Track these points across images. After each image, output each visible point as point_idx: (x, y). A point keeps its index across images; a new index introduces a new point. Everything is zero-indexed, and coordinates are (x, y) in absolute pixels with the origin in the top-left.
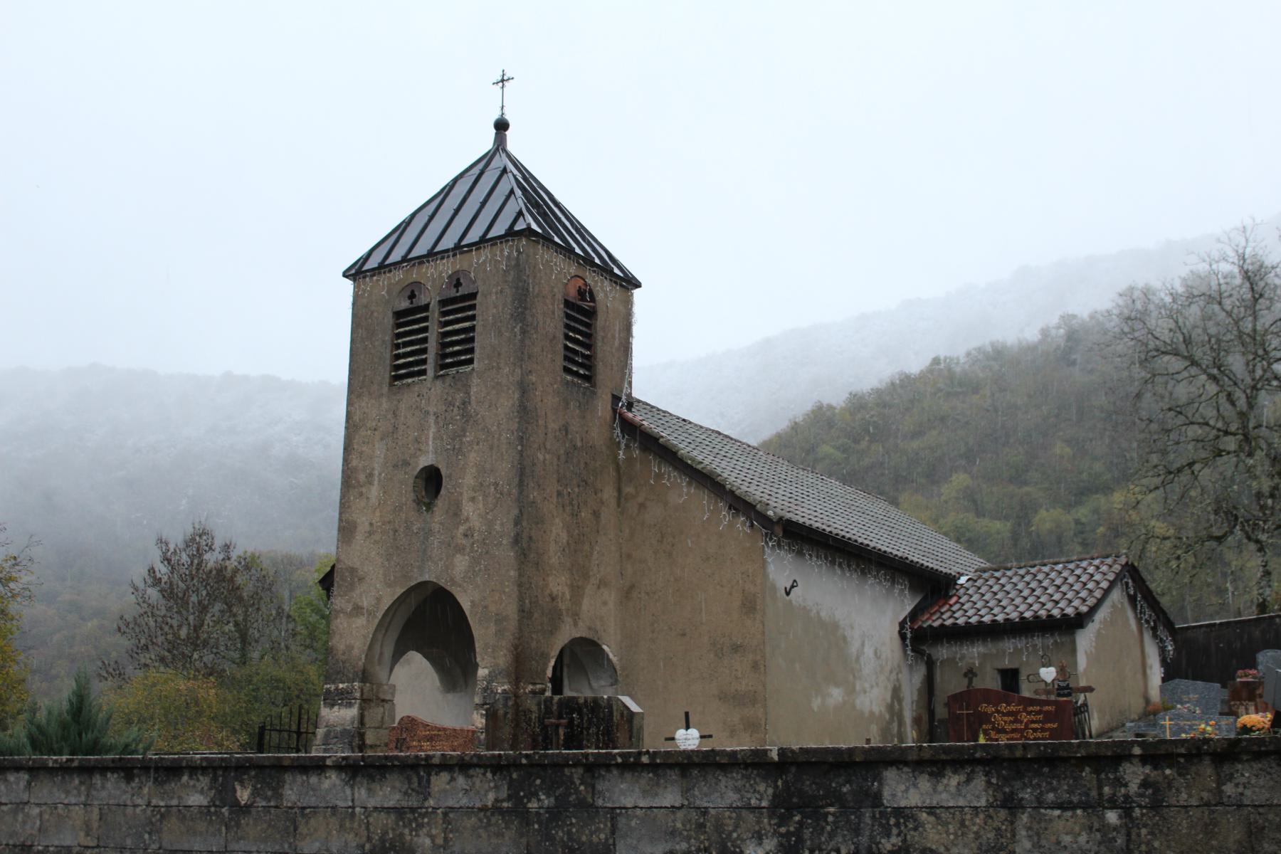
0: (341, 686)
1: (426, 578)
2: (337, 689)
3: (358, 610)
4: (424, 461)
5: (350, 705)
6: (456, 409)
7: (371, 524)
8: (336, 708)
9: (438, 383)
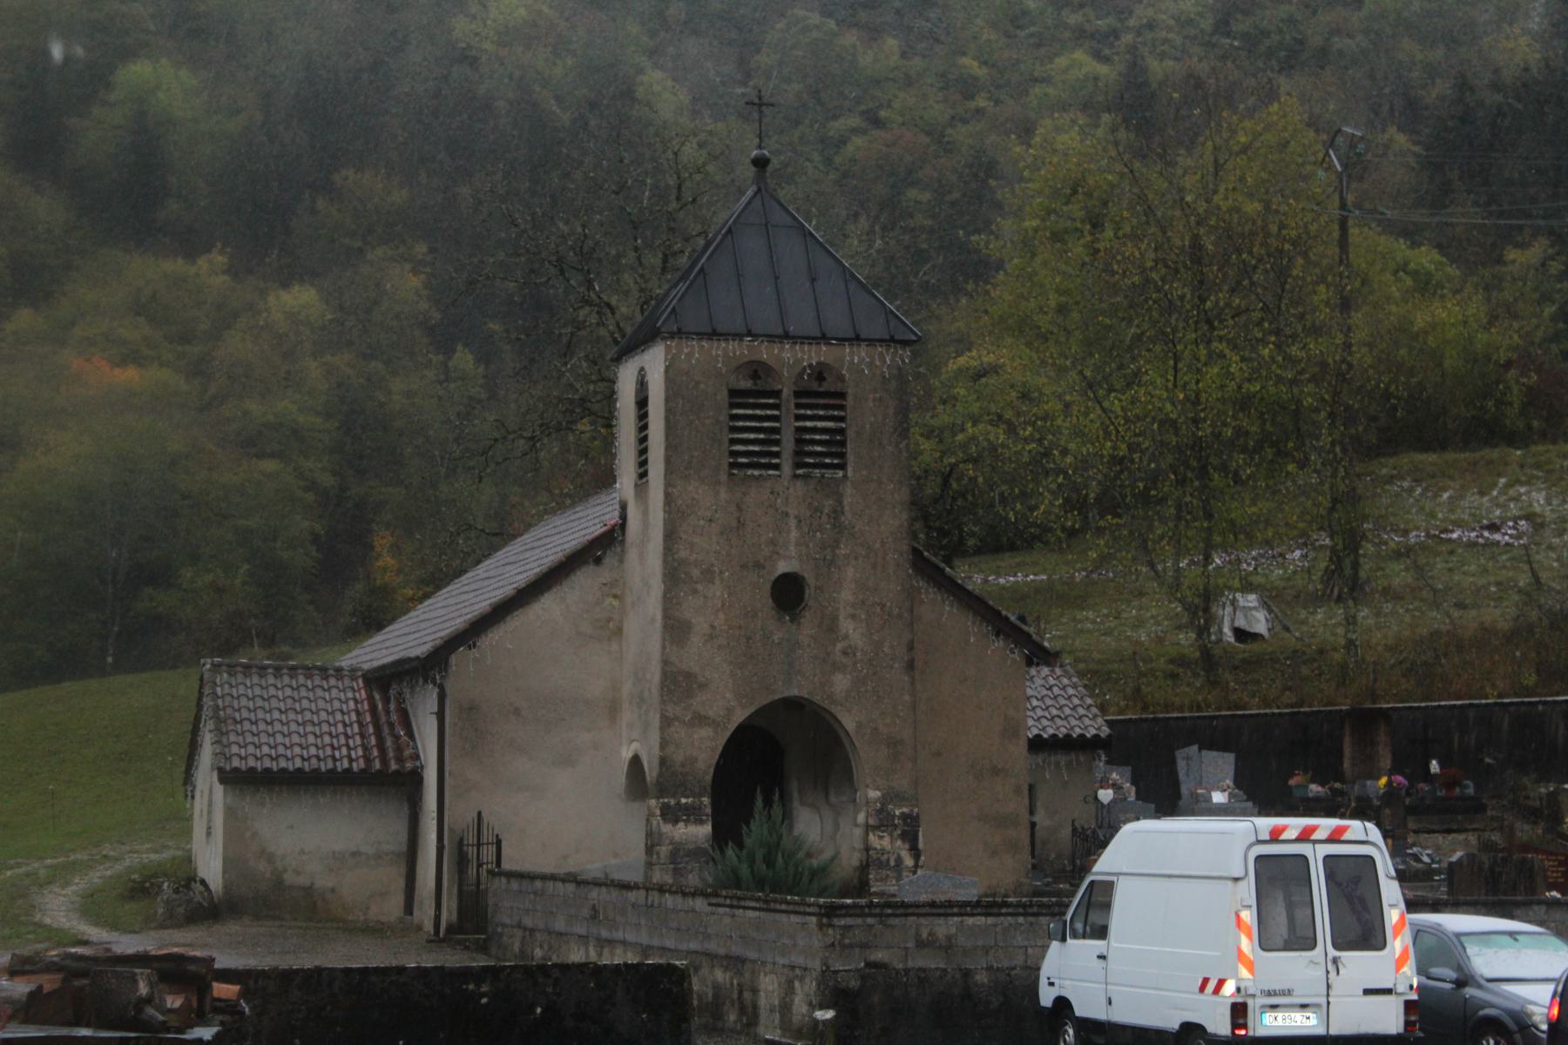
0: (684, 801)
1: (794, 692)
2: (678, 803)
3: (700, 720)
4: (783, 567)
5: (702, 822)
6: (824, 518)
7: (712, 627)
8: (681, 825)
9: (799, 483)
